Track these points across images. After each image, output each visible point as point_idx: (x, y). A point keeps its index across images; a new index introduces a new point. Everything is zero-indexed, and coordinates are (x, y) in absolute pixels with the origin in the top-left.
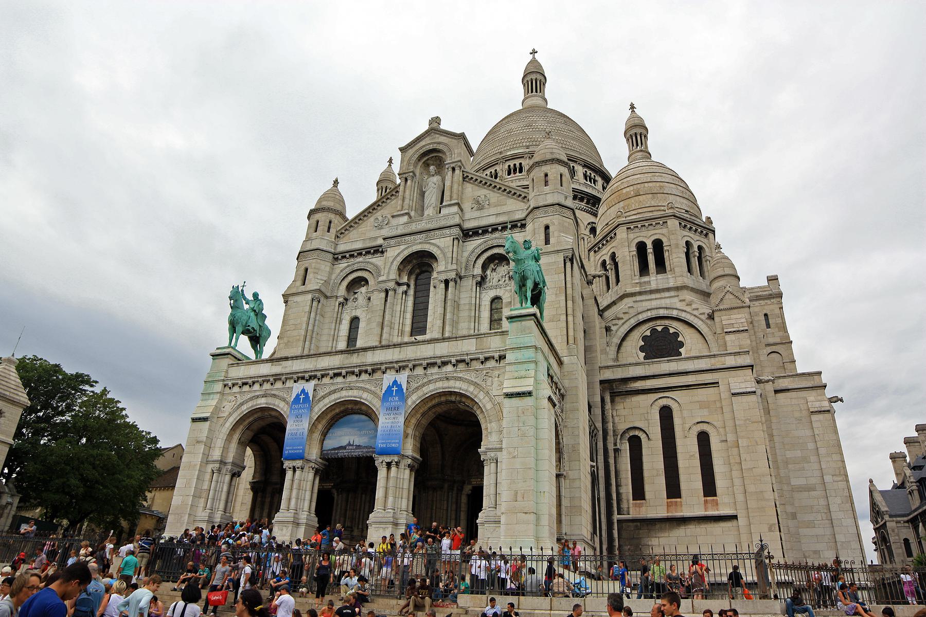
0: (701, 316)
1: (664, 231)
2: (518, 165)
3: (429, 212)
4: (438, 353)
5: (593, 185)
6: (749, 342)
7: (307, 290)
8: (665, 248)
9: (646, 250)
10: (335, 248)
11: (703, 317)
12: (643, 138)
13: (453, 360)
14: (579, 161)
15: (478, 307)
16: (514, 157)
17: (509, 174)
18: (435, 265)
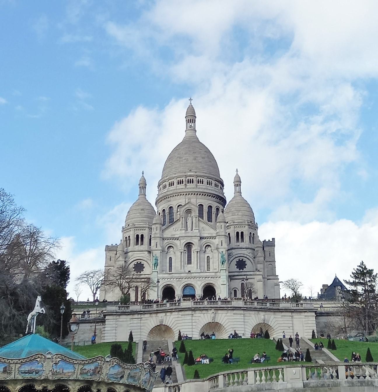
0: (252, 257)
1: (244, 229)
2: (192, 180)
3: (189, 229)
4: (207, 275)
5: (217, 188)
6: (262, 267)
7: (158, 249)
8: (244, 235)
9: (239, 235)
10: (163, 236)
11: (253, 258)
12: (240, 186)
13: (211, 277)
14: (214, 179)
15: (204, 258)
16: (190, 176)
17: (188, 183)
18: (193, 246)
